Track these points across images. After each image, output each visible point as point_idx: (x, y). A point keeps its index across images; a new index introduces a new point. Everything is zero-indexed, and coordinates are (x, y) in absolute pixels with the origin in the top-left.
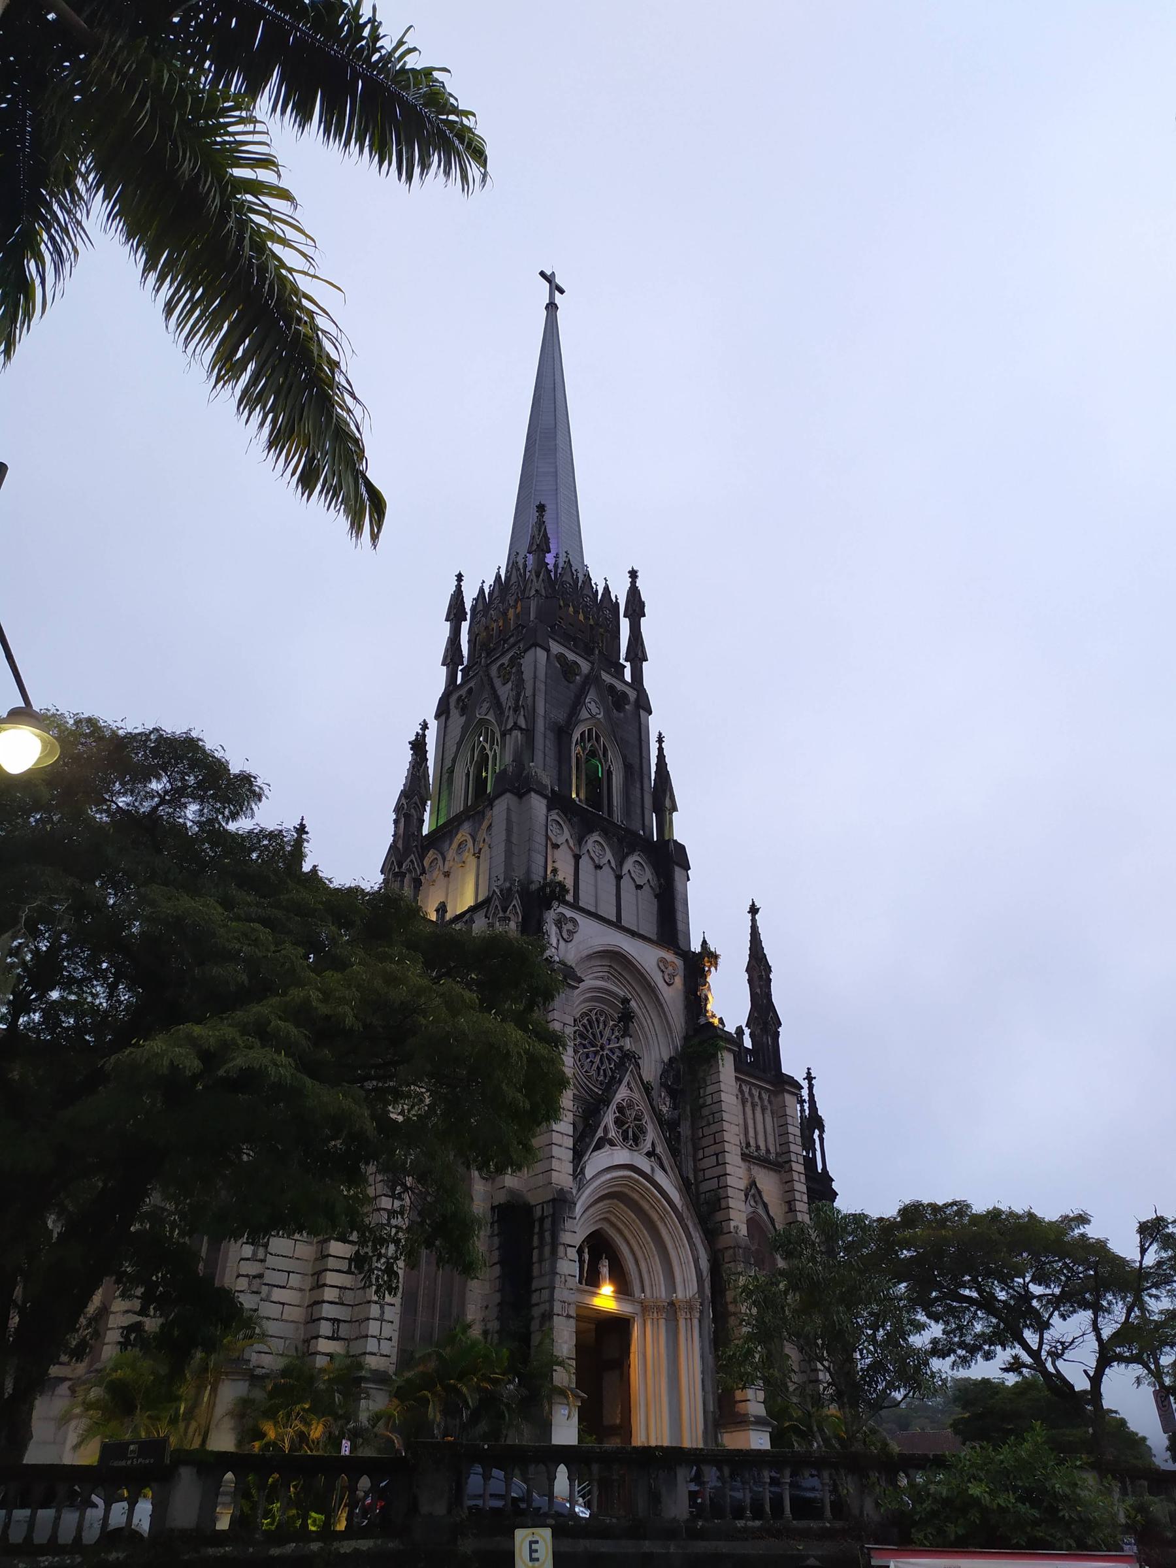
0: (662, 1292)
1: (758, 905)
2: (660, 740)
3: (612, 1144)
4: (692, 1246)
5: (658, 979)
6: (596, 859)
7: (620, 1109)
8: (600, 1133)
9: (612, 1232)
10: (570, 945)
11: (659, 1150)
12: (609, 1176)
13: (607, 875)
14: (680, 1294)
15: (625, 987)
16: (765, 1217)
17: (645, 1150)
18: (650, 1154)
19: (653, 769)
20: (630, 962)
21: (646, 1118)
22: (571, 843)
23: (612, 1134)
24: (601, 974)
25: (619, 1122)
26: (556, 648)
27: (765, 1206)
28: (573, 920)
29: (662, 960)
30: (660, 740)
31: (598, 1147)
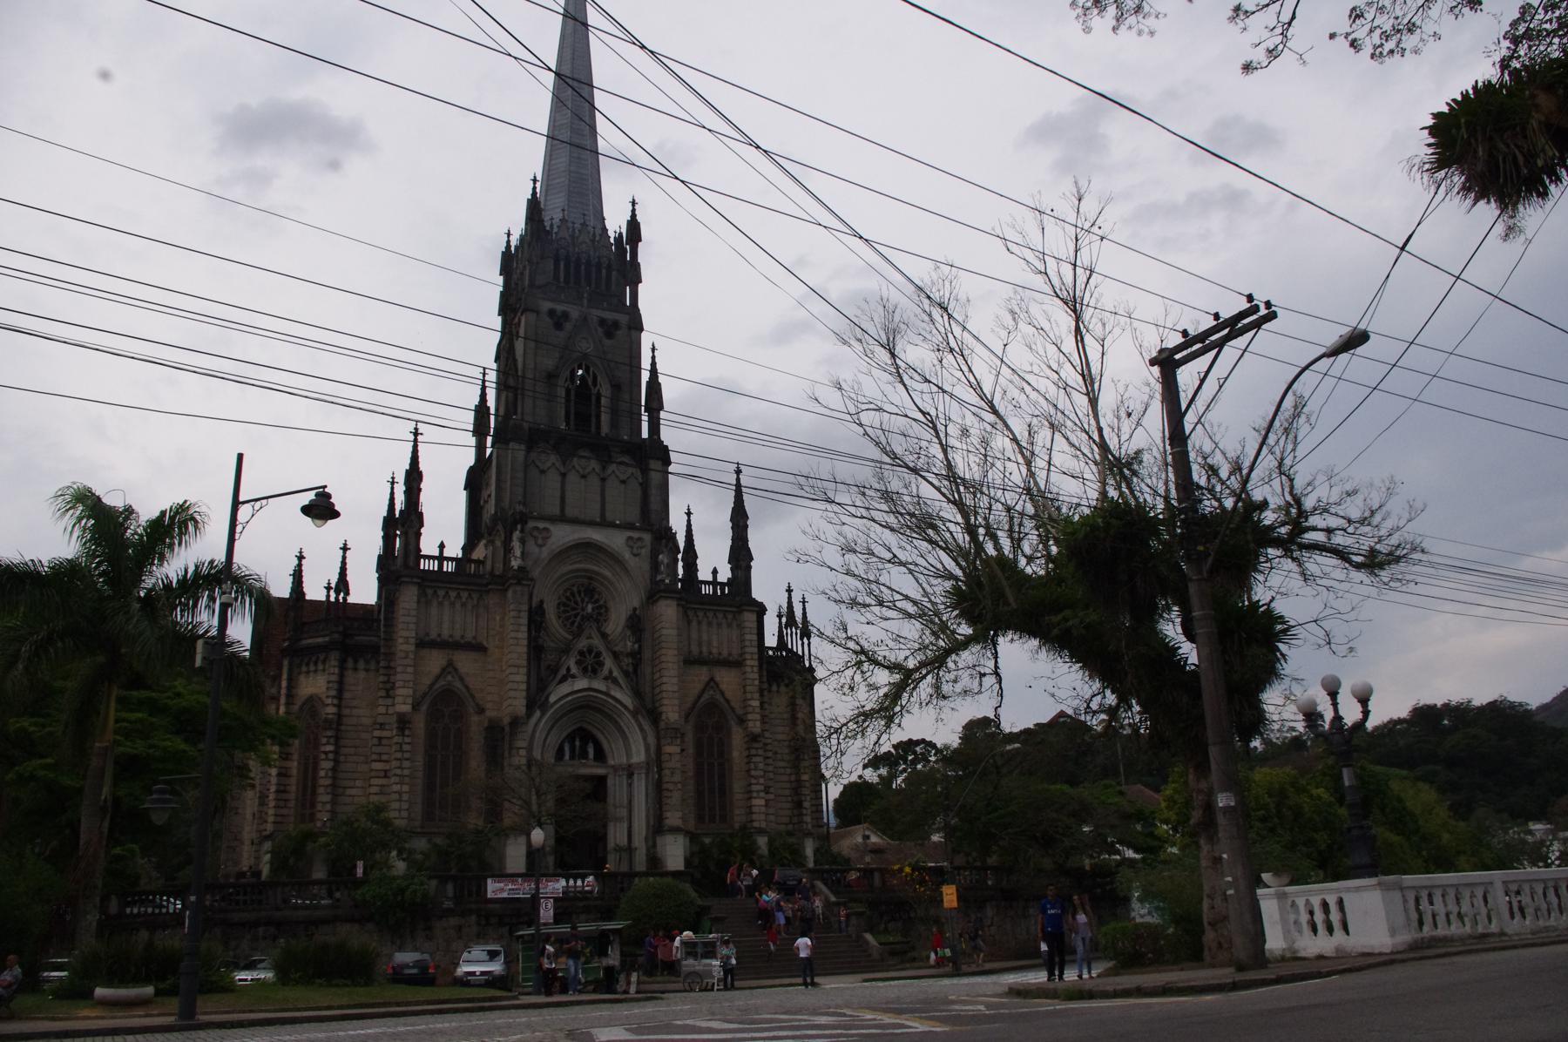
0: (624, 760)
2: (653, 350)
3: (573, 677)
4: (642, 730)
5: (627, 555)
6: (581, 470)
7: (581, 653)
8: (563, 671)
9: (590, 728)
10: (544, 549)
11: (615, 674)
12: (570, 698)
13: (594, 481)
14: (635, 760)
16: (722, 700)
17: (602, 676)
18: (606, 678)
19: (645, 376)
20: (596, 545)
21: (604, 654)
22: (557, 464)
23: (574, 670)
25: (578, 663)
26: (546, 305)
27: (722, 693)
28: (546, 529)
29: (630, 538)
30: (653, 350)
31: (561, 682)
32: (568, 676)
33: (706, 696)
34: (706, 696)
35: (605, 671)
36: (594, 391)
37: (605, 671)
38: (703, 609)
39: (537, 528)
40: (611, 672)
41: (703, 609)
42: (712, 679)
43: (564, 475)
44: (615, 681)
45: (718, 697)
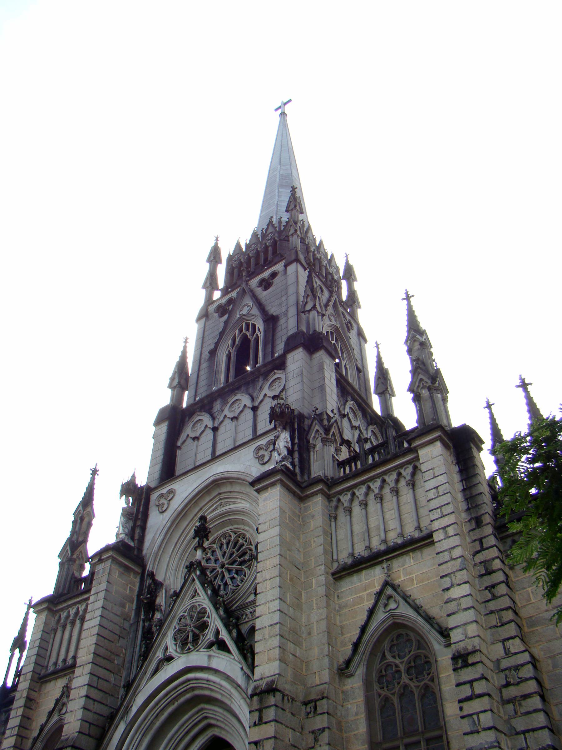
1: (410, 294)
15: (237, 498)
16: (410, 613)
24: (215, 506)
29: (259, 448)
32: (169, 659)
33: (380, 616)
34: (380, 616)
35: (210, 636)
36: (252, 340)
37: (210, 636)
38: (363, 483)
39: (162, 496)
40: (217, 632)
41: (363, 483)
42: (386, 584)
43: (215, 430)
44: (222, 646)
45: (406, 611)
